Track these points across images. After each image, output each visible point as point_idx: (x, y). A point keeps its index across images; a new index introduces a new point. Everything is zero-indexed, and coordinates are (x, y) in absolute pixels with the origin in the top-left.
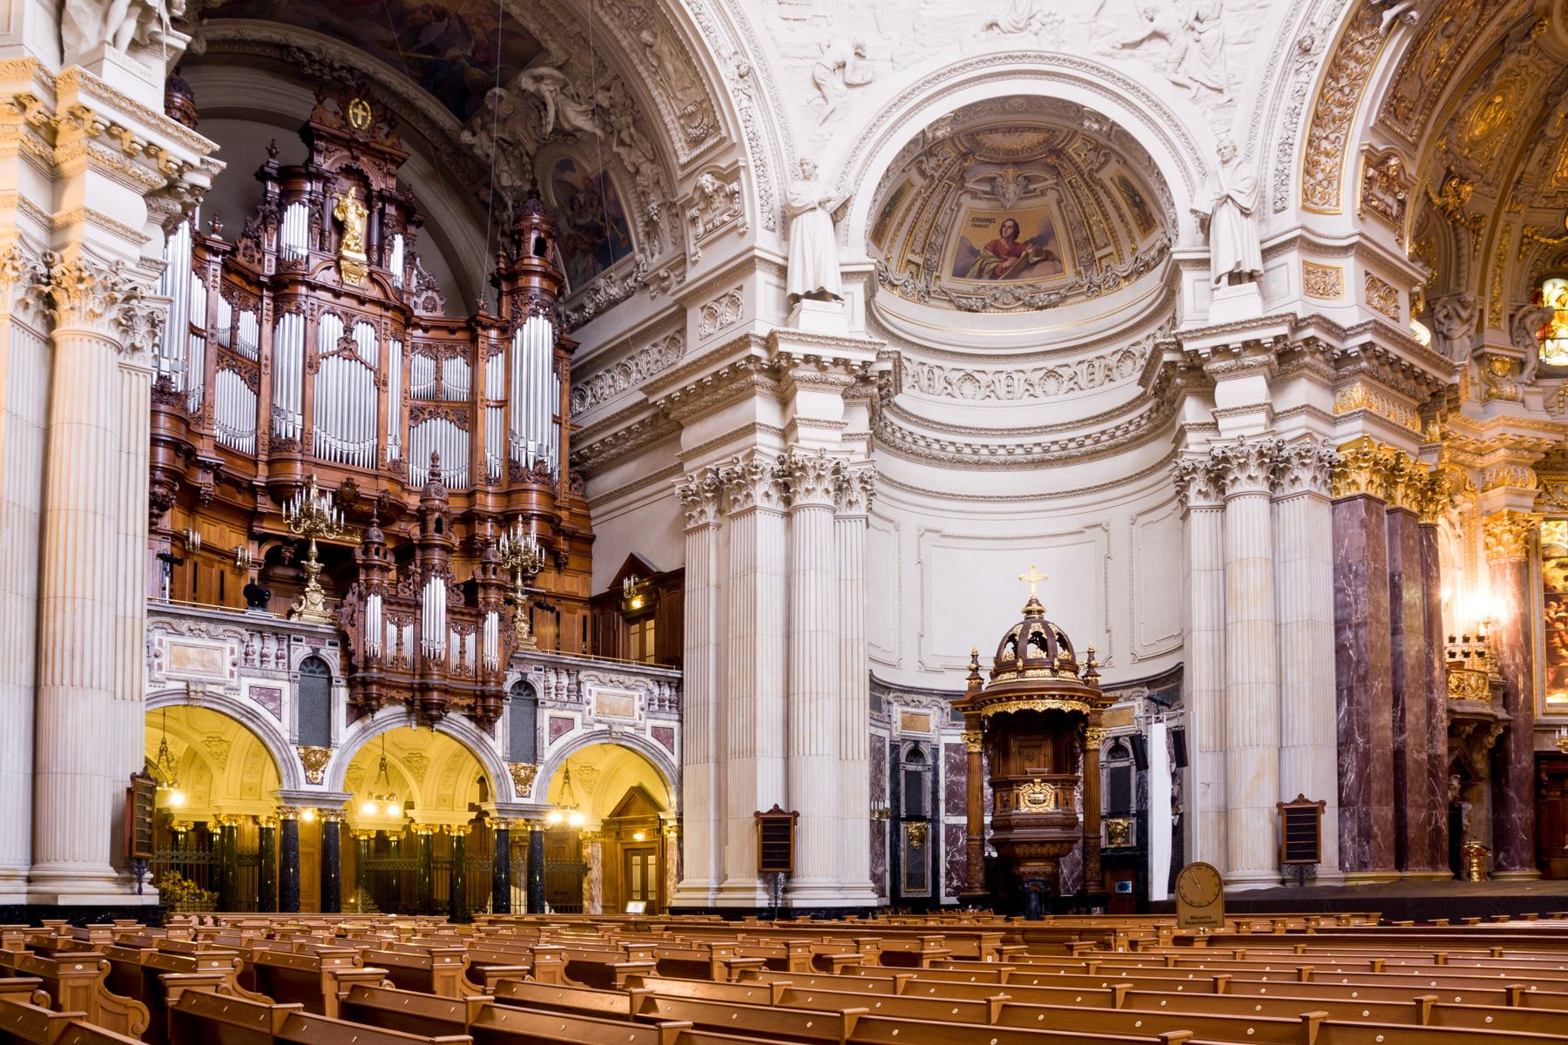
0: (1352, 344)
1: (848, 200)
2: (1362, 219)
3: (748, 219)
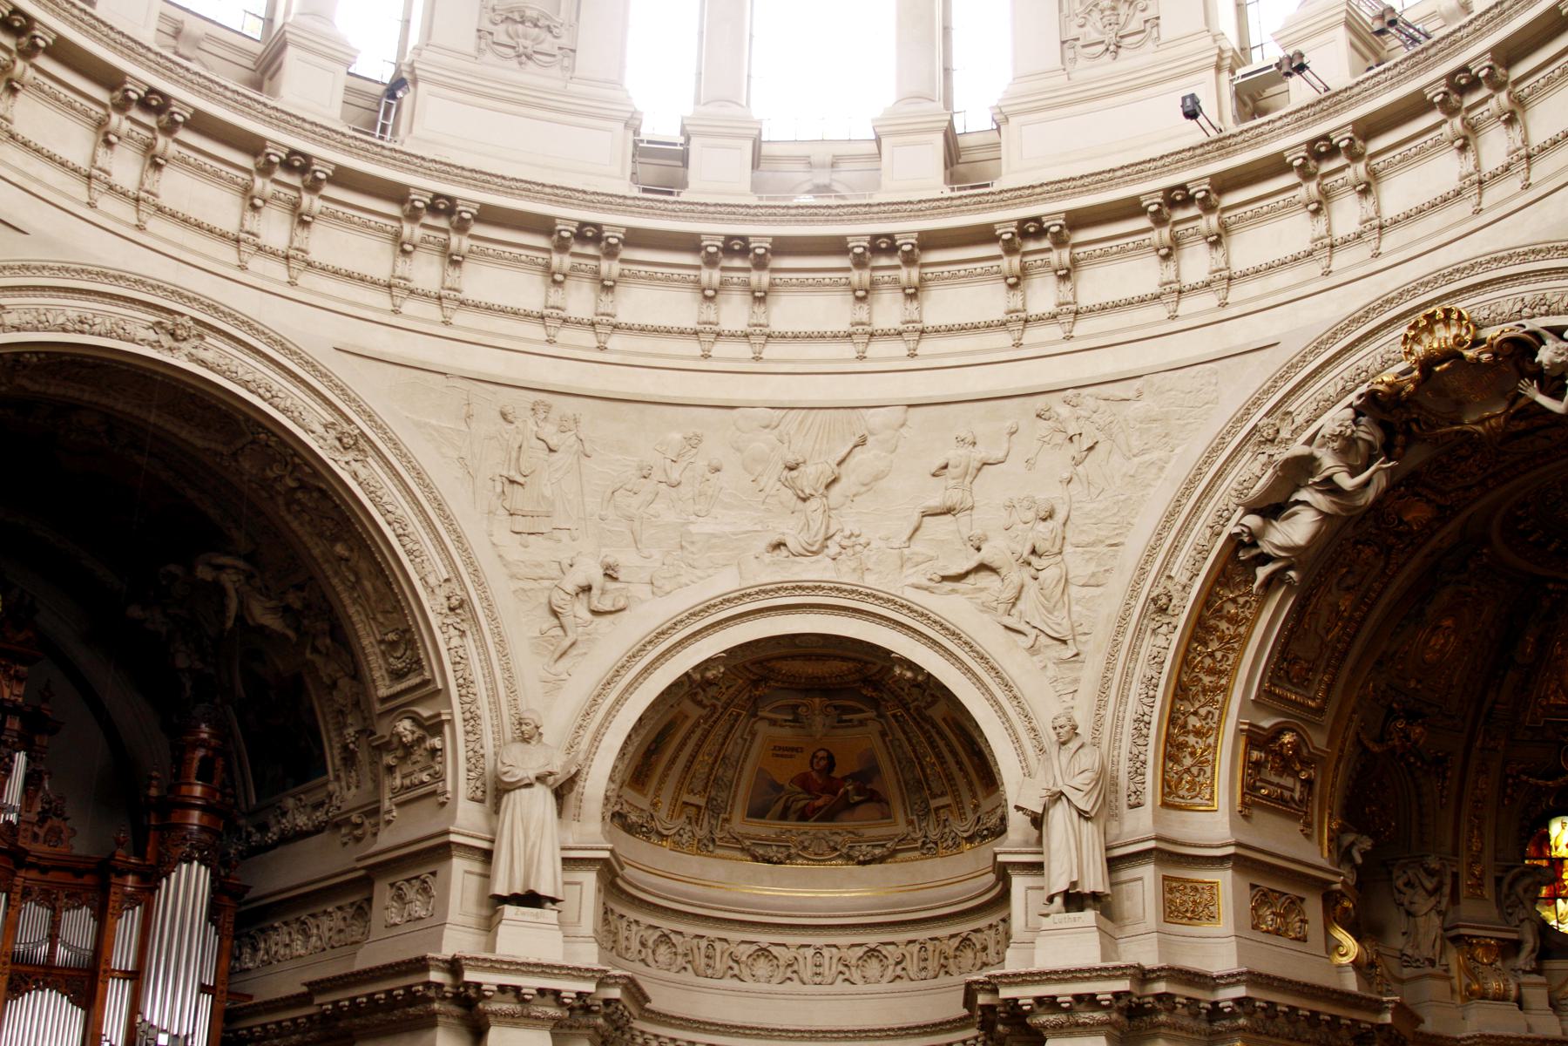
0: (1227, 995)
1: (577, 773)
2: (1245, 817)
3: (449, 787)
